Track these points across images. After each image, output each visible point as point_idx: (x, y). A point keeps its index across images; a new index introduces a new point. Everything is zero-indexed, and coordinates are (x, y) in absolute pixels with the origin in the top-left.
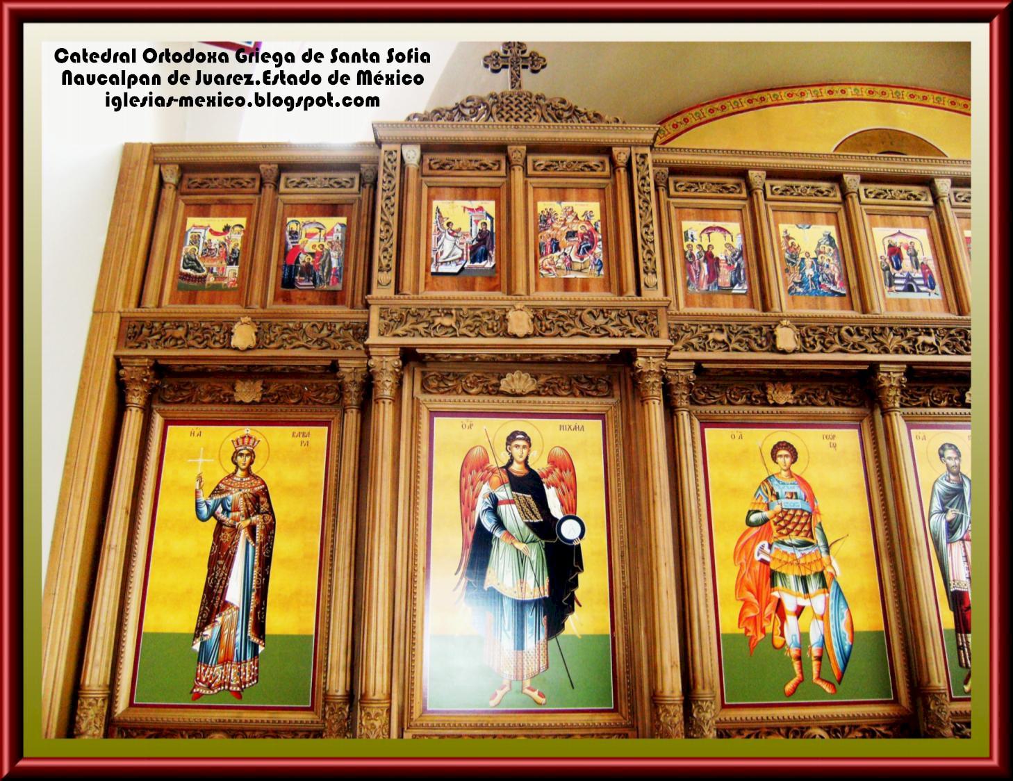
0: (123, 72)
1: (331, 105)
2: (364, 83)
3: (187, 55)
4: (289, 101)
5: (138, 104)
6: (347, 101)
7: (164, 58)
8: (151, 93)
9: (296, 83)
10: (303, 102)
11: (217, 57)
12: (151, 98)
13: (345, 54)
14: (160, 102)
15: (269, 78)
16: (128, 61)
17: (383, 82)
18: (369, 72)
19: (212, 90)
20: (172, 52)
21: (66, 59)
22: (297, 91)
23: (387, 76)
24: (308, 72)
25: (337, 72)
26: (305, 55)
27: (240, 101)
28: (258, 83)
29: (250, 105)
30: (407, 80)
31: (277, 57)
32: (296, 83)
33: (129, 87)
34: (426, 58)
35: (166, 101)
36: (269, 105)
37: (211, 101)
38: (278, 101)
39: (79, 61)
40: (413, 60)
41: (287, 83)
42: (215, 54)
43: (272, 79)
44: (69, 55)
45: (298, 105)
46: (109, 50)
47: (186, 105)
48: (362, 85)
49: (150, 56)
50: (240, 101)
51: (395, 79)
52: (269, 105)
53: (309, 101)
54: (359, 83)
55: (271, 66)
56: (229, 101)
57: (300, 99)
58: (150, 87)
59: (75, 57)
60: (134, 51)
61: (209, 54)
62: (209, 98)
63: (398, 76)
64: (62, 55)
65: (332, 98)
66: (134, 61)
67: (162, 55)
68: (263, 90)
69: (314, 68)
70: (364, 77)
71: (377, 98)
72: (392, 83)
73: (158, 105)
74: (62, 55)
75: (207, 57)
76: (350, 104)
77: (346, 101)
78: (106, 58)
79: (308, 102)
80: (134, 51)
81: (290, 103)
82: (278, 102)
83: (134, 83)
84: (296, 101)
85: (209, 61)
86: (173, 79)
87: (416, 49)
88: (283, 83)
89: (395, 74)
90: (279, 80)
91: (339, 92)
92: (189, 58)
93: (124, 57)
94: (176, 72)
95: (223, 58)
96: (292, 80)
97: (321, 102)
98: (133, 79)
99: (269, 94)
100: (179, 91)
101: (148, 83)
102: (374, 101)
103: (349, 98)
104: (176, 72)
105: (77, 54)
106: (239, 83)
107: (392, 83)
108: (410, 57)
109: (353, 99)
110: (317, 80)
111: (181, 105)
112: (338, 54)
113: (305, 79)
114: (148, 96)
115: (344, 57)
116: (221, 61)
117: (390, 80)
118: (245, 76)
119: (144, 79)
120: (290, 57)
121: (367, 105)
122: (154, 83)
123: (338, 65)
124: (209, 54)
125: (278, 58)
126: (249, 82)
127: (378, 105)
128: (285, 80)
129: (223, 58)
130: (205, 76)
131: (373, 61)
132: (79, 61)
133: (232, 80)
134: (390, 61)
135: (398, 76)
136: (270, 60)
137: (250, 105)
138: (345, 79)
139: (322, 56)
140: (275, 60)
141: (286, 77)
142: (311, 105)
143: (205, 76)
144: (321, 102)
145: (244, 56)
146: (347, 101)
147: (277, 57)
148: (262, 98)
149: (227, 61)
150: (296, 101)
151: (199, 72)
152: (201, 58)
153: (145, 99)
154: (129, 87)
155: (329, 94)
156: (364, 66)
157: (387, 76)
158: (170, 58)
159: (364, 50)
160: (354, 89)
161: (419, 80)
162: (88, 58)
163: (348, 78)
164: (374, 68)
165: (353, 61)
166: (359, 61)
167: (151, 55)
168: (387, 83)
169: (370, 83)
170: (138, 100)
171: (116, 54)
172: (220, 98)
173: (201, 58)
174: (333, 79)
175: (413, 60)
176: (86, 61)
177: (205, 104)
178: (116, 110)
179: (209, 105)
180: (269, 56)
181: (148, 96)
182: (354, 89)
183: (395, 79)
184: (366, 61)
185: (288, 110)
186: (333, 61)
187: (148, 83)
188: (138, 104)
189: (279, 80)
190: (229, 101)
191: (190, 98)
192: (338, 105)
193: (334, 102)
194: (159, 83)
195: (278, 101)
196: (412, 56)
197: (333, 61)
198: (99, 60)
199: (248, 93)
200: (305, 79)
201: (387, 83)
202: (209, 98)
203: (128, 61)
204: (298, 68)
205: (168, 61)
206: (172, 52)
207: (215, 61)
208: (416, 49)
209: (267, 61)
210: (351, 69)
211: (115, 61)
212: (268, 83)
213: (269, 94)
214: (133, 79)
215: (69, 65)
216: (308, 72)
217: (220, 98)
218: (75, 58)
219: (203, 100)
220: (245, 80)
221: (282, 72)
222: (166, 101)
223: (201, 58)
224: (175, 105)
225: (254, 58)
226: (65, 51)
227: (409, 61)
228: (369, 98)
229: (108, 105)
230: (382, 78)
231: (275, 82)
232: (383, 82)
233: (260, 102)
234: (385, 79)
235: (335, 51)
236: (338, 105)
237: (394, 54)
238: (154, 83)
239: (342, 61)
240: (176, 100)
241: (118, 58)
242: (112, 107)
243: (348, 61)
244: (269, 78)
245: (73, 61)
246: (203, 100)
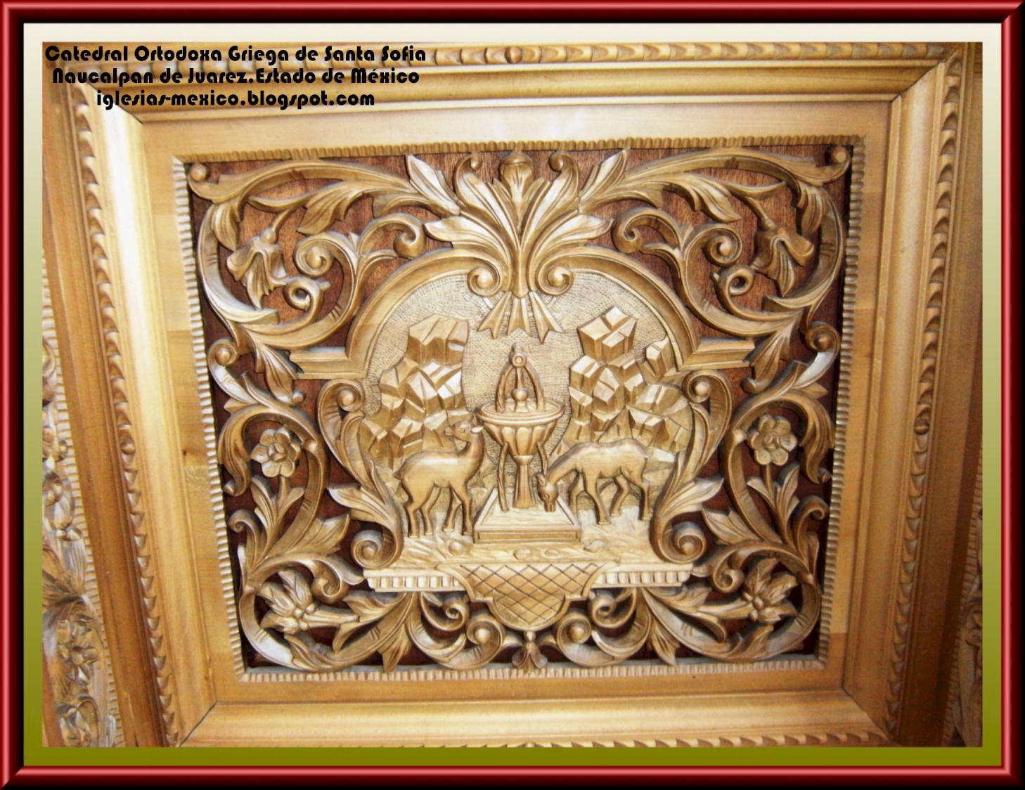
2: (359, 82)
3: (179, 52)
5: (130, 102)
7: (156, 56)
10: (296, 100)
11: (210, 55)
12: (143, 97)
14: (152, 100)
16: (120, 59)
17: (378, 80)
19: (204, 89)
20: (164, 49)
21: (57, 57)
22: (292, 90)
26: (299, 53)
27: (233, 100)
28: (251, 81)
33: (121, 85)
34: (421, 55)
35: (158, 99)
36: (262, 103)
37: (204, 100)
38: (271, 100)
42: (207, 51)
43: (265, 77)
46: (101, 48)
47: (179, 103)
48: (356, 84)
49: (142, 53)
50: (233, 100)
53: (303, 100)
54: (353, 81)
55: (264, 63)
56: (221, 100)
57: (294, 97)
59: (66, 56)
60: (126, 48)
61: (202, 51)
62: (201, 96)
64: (52, 53)
65: (326, 97)
66: (126, 59)
67: (154, 52)
70: (359, 76)
71: (371, 97)
73: (150, 103)
75: (200, 55)
77: (340, 100)
78: (97, 55)
79: (302, 101)
80: (126, 48)
81: (284, 102)
82: (271, 101)
84: (289, 99)
87: (411, 47)
91: (333, 90)
92: (181, 56)
93: (116, 55)
95: (216, 55)
99: (262, 93)
103: (343, 97)
105: (68, 52)
107: (387, 81)
108: (405, 55)
110: (311, 79)
111: (173, 103)
113: (299, 77)
114: (140, 94)
116: (214, 59)
117: (384, 78)
120: (284, 55)
124: (202, 51)
125: (271, 55)
126: (242, 81)
129: (216, 55)
130: (197, 74)
136: (264, 58)
138: (339, 78)
139: (316, 54)
140: (269, 58)
144: (315, 100)
145: (237, 54)
146: (342, 100)
148: (255, 97)
150: (289, 99)
152: (193, 55)
153: (137, 97)
154: (121, 85)
155: (323, 92)
158: (163, 56)
159: (359, 48)
160: (349, 89)
161: (414, 78)
162: (79, 55)
167: (142, 52)
168: (382, 81)
169: (364, 81)
170: (130, 99)
171: (108, 52)
172: (213, 97)
173: (193, 55)
174: (327, 79)
176: (77, 59)
177: (197, 102)
178: (108, 108)
179: (201, 103)
180: (262, 54)
181: (140, 94)
186: (327, 59)
188: (130, 102)
190: (221, 100)
191: (183, 97)
192: (332, 103)
193: (328, 100)
195: (271, 100)
196: (408, 54)
198: (90, 58)
200: (299, 77)
201: (382, 81)
202: (201, 96)
203: (120, 59)
204: (293, 64)
205: (160, 58)
206: (164, 49)
207: (207, 59)
211: (107, 59)
212: (262, 81)
213: (262, 93)
217: (213, 97)
219: (196, 99)
220: (238, 78)
222: (158, 99)
223: (193, 55)
224: (167, 103)
225: (247, 55)
228: (363, 96)
229: (99, 103)
231: (268, 80)
232: (378, 80)
233: (253, 100)
237: (389, 53)
240: (168, 99)
242: (104, 106)
246: (196, 99)
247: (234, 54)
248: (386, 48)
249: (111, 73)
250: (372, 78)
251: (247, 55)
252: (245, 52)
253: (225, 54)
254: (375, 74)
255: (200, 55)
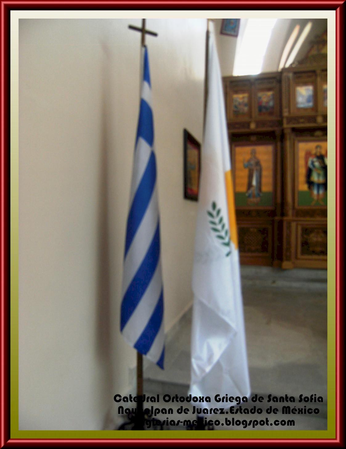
0: (152, 407)
1: (268, 424)
2: (286, 413)
4: (245, 423)
6: (277, 423)
7: (175, 400)
8: (167, 418)
9: (248, 413)
10: (252, 423)
11: (204, 399)
13: (276, 397)
15: (233, 410)
16: (155, 401)
17: (297, 412)
18: (289, 407)
20: (179, 396)
21: (120, 400)
22: (248, 417)
23: (299, 409)
24: (255, 407)
25: (271, 407)
27: (217, 423)
29: (223, 424)
30: (310, 411)
31: (238, 399)
32: (248, 413)
35: (176, 422)
36: (233, 425)
39: (127, 401)
40: (313, 401)
41: (243, 413)
42: (203, 397)
43: (235, 411)
44: (122, 398)
45: (249, 424)
48: (285, 415)
51: (303, 411)
52: (233, 425)
54: (283, 413)
57: (251, 421)
58: (167, 415)
60: (158, 396)
63: (305, 409)
64: (118, 398)
66: (158, 401)
67: (174, 398)
68: (230, 417)
69: (258, 404)
70: (286, 410)
71: (293, 421)
72: (302, 413)
74: (118, 398)
75: (199, 399)
76: (278, 424)
77: (276, 423)
80: (158, 396)
82: (238, 423)
83: (158, 413)
84: (248, 423)
85: (200, 401)
86: (180, 411)
87: (315, 395)
88: (241, 413)
89: (304, 408)
90: (239, 411)
91: (272, 418)
94: (182, 407)
96: (246, 411)
97: (262, 423)
98: (157, 411)
99: (233, 419)
100: (182, 417)
101: (166, 413)
102: (292, 423)
103: (278, 421)
104: (182, 407)
106: (216, 413)
108: (312, 399)
109: (280, 422)
110: (260, 411)
112: (272, 398)
113: (253, 410)
115: (275, 399)
117: (300, 411)
118: (220, 409)
119: (164, 411)
121: (288, 425)
122: (169, 413)
123: (272, 403)
124: (200, 397)
127: (294, 425)
128: (242, 411)
130: (198, 409)
131: (291, 401)
132: (127, 401)
133: (212, 411)
134: (300, 401)
135: (305, 409)
137: (223, 424)
138: (275, 411)
140: (237, 401)
141: (243, 410)
142: (257, 425)
143: (198, 409)
146: (277, 423)
147: (238, 399)
148: (229, 421)
149: (210, 401)
150: (248, 423)
151: (194, 407)
155: (267, 419)
156: (286, 404)
157: (299, 409)
158: (178, 399)
159: (286, 395)
163: (277, 410)
164: (292, 405)
165: (280, 401)
166: (283, 401)
168: (299, 413)
169: (289, 413)
171: (148, 398)
174: (269, 411)
175: (313, 401)
176: (131, 401)
180: (233, 399)
181: (166, 420)
182: (280, 417)
183: (303, 411)
184: (287, 401)
185: (244, 427)
186: (269, 401)
187: (166, 413)
189: (239, 411)
192: (271, 424)
193: (269, 423)
194: (172, 413)
197: (269, 401)
199: (222, 418)
201: (299, 413)
205: (177, 401)
206: (179, 396)
208: (315, 395)
209: (232, 401)
210: (280, 405)
212: (233, 413)
213: (233, 419)
214: (157, 411)
215: (122, 404)
216: (255, 407)
218: (125, 399)
220: (220, 411)
221: (240, 407)
222: (176, 422)
225: (225, 400)
226: (120, 396)
227: (311, 401)
228: (289, 421)
230: (296, 410)
231: (236, 413)
232: (297, 412)
233: (228, 423)
234: (298, 411)
235: (270, 396)
236: (271, 424)
238: (169, 413)
239: (274, 401)
241: (149, 399)
243: (277, 401)
244: (233, 410)
245: (124, 401)
247: (218, 399)
248: (301, 396)
249: (150, 408)
250: (294, 411)
251: (225, 400)
252: (224, 398)
253: (213, 399)
254: (295, 409)
255: (199, 399)
